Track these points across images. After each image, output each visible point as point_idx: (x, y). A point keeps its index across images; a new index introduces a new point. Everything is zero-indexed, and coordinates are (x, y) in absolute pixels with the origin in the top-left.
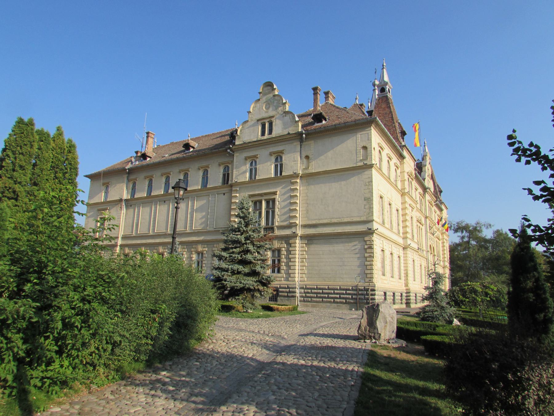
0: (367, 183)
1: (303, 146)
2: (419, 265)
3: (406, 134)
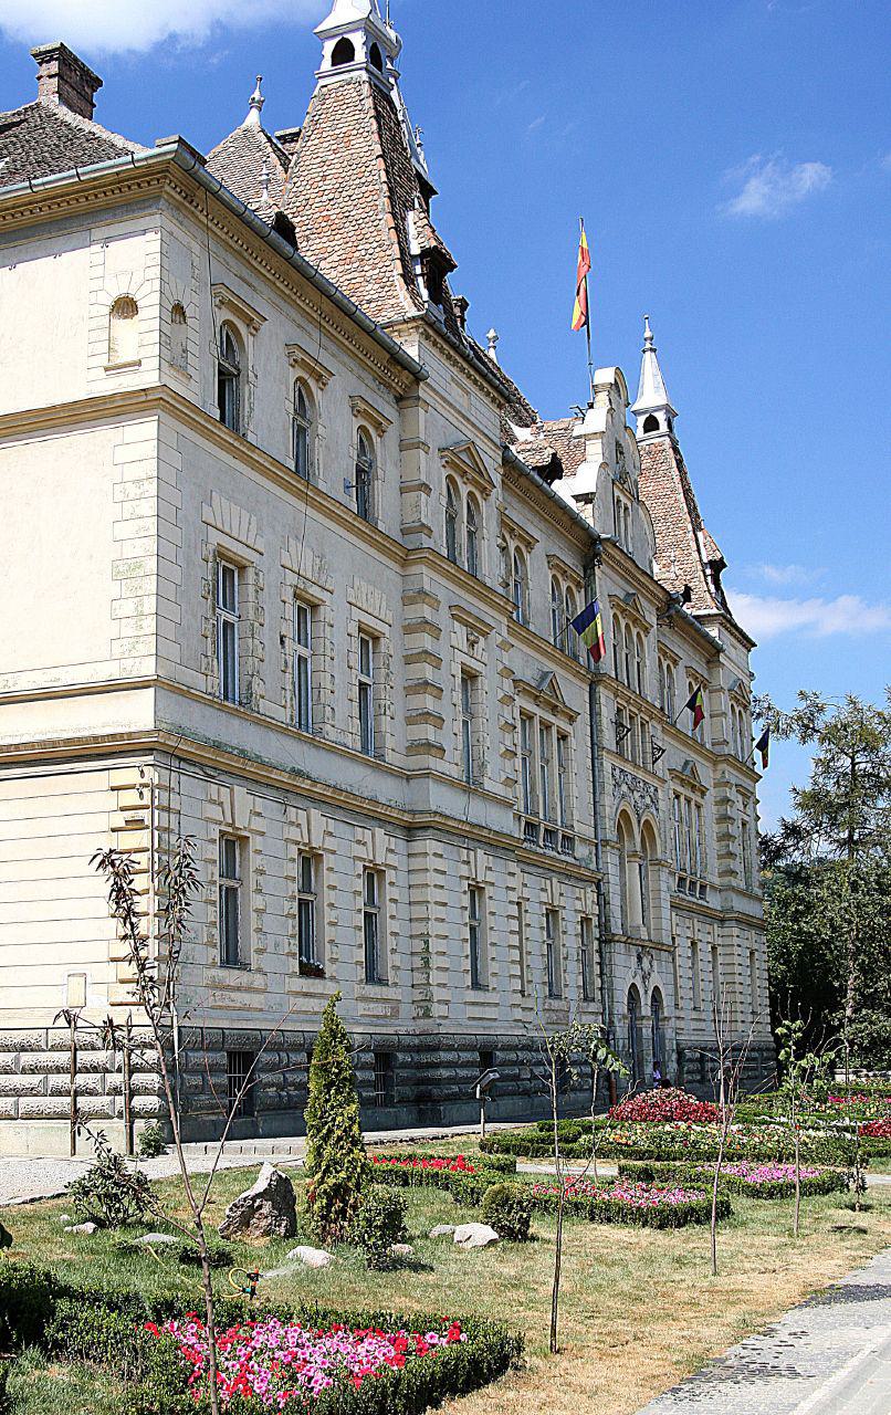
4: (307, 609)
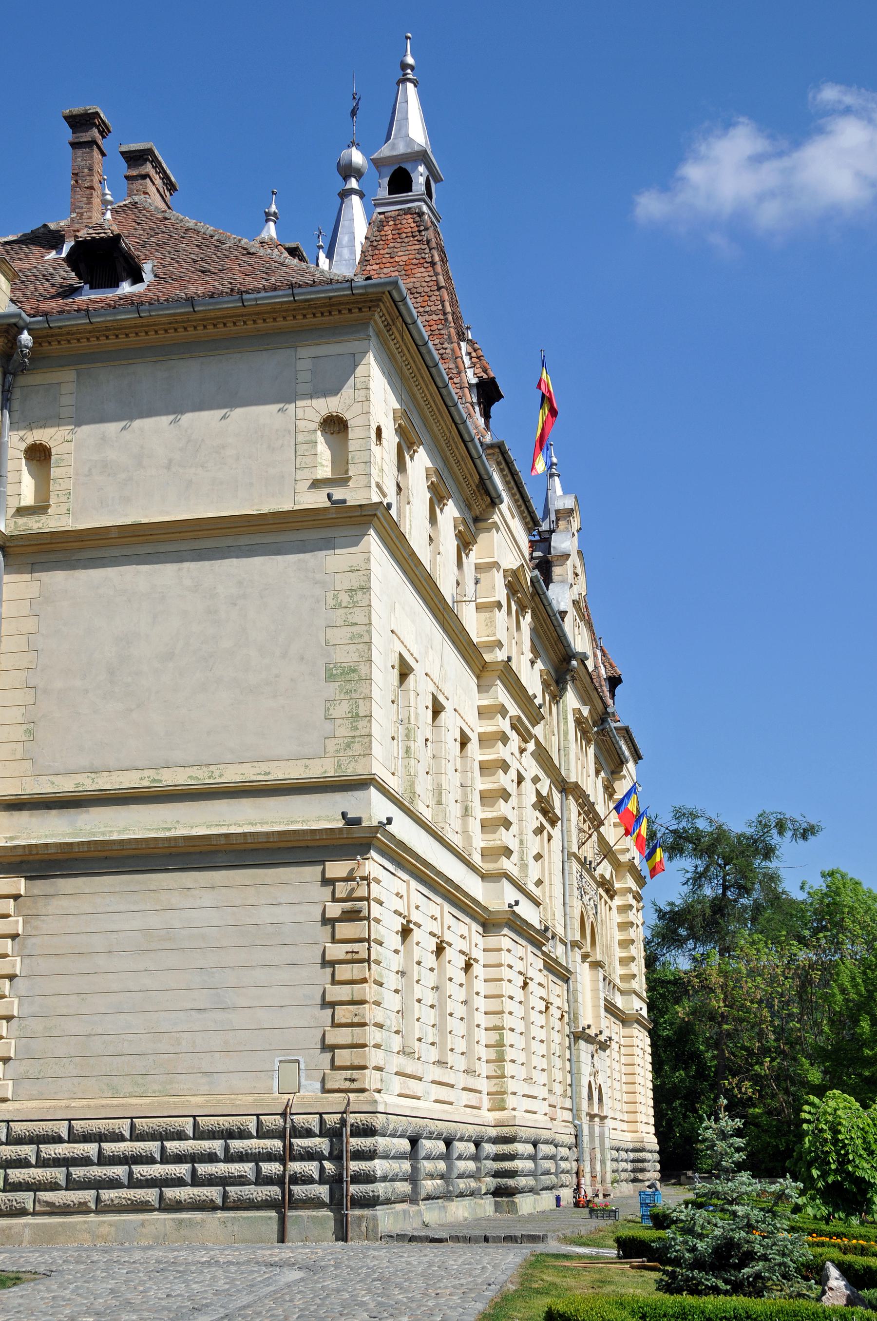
0: (345, 598)
1: (17, 394)
2: (542, 1006)
3: (500, 396)
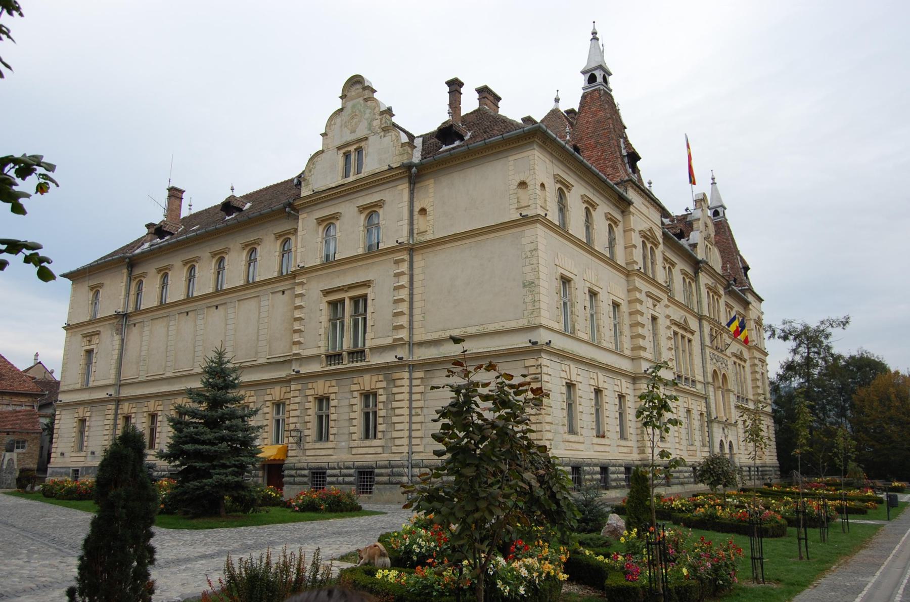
0: (529, 254)
4: (593, 294)
